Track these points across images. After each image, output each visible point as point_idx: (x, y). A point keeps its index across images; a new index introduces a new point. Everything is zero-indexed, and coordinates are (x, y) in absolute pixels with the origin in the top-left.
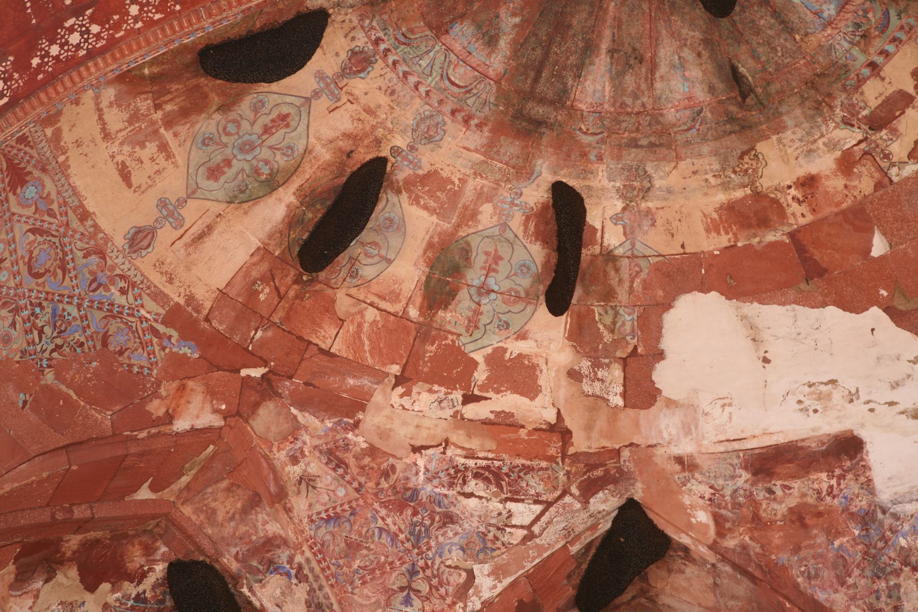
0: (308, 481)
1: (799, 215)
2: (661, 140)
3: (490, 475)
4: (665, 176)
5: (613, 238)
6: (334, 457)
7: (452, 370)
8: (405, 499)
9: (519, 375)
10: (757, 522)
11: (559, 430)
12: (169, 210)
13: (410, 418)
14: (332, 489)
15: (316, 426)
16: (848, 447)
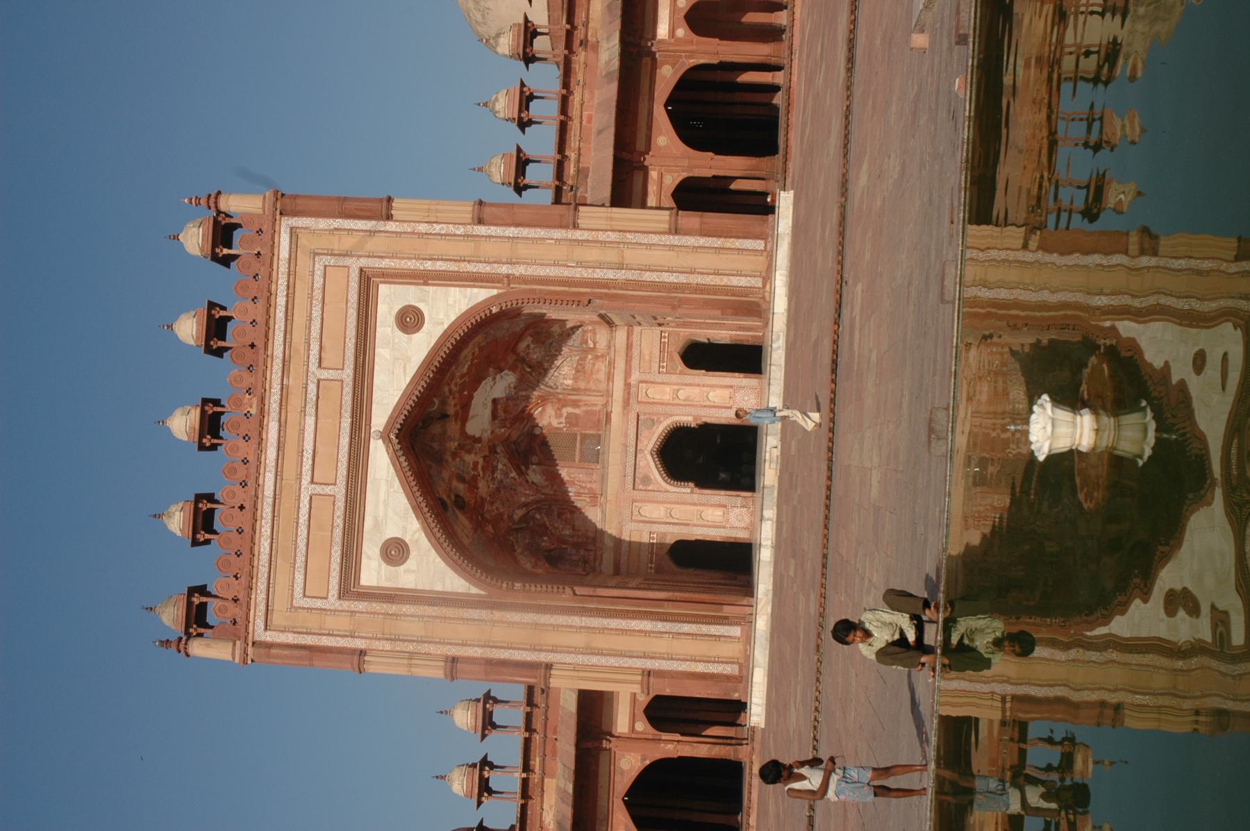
2: (444, 432)
3: (493, 472)
6: (492, 503)
7: (475, 478)
8: (498, 489)
9: (476, 464)
10: (505, 419)
11: (484, 457)
13: (483, 488)
14: (498, 504)
15: (487, 507)
16: (495, 401)
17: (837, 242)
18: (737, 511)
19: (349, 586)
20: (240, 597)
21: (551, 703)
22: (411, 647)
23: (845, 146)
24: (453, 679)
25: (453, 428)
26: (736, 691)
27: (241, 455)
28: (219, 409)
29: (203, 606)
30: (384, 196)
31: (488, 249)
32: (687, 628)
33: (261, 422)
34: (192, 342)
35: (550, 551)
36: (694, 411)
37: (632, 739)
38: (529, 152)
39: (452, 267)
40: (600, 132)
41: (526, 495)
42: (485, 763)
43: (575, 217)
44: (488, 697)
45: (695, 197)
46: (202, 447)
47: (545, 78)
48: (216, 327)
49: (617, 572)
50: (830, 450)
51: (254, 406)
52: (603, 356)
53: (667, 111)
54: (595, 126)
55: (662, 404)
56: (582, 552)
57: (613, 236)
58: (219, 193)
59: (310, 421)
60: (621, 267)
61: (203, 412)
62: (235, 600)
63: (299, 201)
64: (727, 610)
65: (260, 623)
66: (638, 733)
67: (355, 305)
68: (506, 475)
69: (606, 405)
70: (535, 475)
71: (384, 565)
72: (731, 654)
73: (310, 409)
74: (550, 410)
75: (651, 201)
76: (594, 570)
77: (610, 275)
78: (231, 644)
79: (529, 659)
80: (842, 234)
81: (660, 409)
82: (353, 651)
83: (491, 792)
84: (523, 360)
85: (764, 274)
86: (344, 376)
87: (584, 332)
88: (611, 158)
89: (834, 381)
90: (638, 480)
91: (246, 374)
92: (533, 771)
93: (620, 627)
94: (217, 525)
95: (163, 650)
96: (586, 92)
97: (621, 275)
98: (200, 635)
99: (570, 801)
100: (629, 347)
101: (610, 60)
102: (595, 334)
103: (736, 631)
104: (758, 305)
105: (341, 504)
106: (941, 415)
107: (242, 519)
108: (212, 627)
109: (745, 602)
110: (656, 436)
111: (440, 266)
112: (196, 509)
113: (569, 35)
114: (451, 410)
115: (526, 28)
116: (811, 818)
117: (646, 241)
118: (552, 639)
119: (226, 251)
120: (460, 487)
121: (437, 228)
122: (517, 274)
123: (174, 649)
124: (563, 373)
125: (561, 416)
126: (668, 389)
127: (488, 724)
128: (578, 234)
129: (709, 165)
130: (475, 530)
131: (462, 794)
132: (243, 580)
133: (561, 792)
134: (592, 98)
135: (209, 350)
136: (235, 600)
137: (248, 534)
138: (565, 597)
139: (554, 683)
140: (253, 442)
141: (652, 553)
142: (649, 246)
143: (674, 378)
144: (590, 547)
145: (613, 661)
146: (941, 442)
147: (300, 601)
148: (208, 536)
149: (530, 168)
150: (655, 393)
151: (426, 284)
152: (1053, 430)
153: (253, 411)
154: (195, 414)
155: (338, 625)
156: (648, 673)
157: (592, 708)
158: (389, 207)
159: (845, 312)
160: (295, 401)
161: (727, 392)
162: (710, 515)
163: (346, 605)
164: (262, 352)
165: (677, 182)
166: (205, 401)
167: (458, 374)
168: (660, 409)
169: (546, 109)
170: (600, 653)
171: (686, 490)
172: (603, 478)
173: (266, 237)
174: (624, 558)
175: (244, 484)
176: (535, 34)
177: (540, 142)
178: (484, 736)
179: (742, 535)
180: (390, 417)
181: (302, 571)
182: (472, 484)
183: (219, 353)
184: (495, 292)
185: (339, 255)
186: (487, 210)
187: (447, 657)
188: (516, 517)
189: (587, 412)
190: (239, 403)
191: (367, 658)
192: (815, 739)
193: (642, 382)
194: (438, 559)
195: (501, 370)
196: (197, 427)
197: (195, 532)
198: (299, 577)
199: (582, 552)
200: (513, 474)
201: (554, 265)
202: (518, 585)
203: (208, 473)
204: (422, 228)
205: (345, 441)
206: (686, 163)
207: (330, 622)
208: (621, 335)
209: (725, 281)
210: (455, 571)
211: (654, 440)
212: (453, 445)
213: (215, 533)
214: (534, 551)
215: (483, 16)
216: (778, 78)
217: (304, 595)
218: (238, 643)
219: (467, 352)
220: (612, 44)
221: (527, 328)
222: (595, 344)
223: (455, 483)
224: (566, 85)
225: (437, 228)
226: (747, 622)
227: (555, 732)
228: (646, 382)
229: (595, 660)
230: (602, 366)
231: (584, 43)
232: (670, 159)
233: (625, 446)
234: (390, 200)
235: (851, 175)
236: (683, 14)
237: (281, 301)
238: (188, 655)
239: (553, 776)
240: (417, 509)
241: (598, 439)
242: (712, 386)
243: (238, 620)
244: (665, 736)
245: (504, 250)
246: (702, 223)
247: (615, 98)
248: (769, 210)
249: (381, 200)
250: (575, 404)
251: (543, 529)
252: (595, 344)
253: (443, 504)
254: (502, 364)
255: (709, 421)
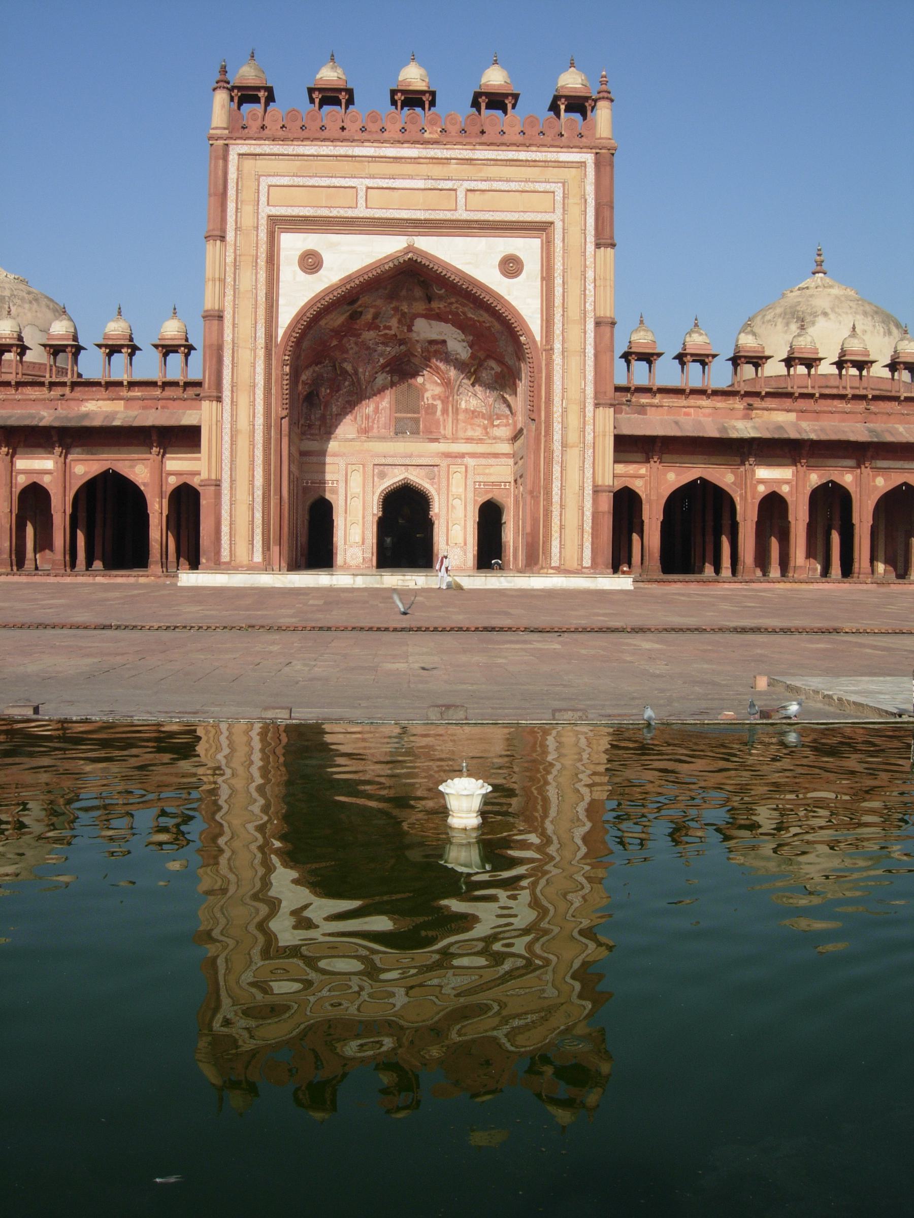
0: (352, 348)
1: (438, 311)
2: (415, 300)
3: (383, 343)
4: (415, 304)
5: (406, 310)
6: (356, 343)
7: (377, 328)
8: (368, 348)
9: (389, 328)
10: (428, 351)
11: (395, 335)
12: (332, 319)
13: (369, 336)
14: (356, 349)
15: (353, 339)
16: (444, 342)
17: (594, 626)
18: (360, 554)
19: (278, 225)
20: (266, 131)
21: (188, 402)
22: (229, 280)
23: (673, 630)
24: (204, 317)
25: (420, 307)
26: (207, 560)
27: (388, 126)
28: (427, 106)
29: (255, 100)
30: (616, 241)
31: (574, 333)
32: (258, 516)
33: (417, 142)
34: (483, 81)
35: (318, 395)
36: (443, 513)
37: (161, 474)
38: (658, 363)
39: (558, 301)
40: (676, 423)
41: (364, 372)
42: (134, 349)
43: (605, 405)
44: (190, 348)
45: (626, 505)
46: (393, 93)
47: (720, 375)
48: (497, 101)
49: (303, 454)
50: (419, 629)
51: (431, 136)
52: (487, 433)
53: (696, 480)
54: (682, 419)
55: (448, 486)
56: (318, 423)
57: (589, 438)
58: (612, 101)
59: (420, 184)
60: (564, 445)
61: (423, 92)
62: (263, 127)
63: (608, 168)
64: (275, 550)
65: (244, 149)
66: (167, 479)
67: (521, 219)
68: (381, 355)
69: (445, 437)
70: (382, 378)
71: (299, 253)
72: (238, 554)
73: (430, 184)
74: (438, 390)
75: (621, 468)
76: (303, 433)
77: (557, 437)
78: (225, 125)
79: (225, 382)
80: (600, 630)
81: (444, 483)
82: (223, 230)
83: (109, 355)
84: (480, 365)
85: (562, 567)
86: (460, 212)
87: (507, 417)
88: (655, 433)
89: (477, 629)
90: (381, 468)
91: (458, 127)
92: (129, 390)
93: (256, 459)
94: (326, 108)
95: (219, 69)
96: (710, 411)
97: (557, 446)
98: (232, 99)
99: (106, 423)
100: (496, 455)
101: (737, 430)
102: (506, 426)
103: (258, 557)
104: (536, 563)
105: (350, 213)
106: (461, 714)
107: (333, 130)
108: (239, 108)
109: (284, 564)
110: (421, 482)
111: (558, 291)
112: (339, 90)
113: (757, 394)
114: (435, 305)
115: (761, 358)
116: (110, 627)
117: (586, 466)
118: (243, 401)
119: (563, 107)
120: (368, 316)
121: (590, 287)
122: (554, 357)
123: (218, 77)
124: (474, 398)
125: (434, 399)
126: (461, 490)
127: (167, 350)
128: (590, 407)
129: (652, 517)
130: (332, 330)
131: (107, 330)
132: (281, 133)
133: (113, 415)
134: (705, 415)
135: (477, 95)
136: (263, 127)
137: (321, 135)
138: (279, 410)
139: (205, 404)
140: (399, 136)
141: (320, 483)
142: (582, 469)
143: (470, 495)
144: (322, 429)
145: (226, 454)
146: (439, 715)
147: (264, 182)
148: (317, 101)
149: (644, 365)
150: (457, 480)
151: (543, 279)
152: (464, 799)
153: (427, 135)
154: (422, 86)
155: (246, 216)
156: (218, 484)
157: (187, 438)
158: (607, 246)
159: (536, 636)
160: (437, 170)
161: (460, 540)
162: (355, 530)
163: (263, 222)
164: (478, 140)
165: (637, 491)
166: (433, 94)
167: (466, 309)
168: (444, 483)
169: (694, 376)
170: (233, 442)
171: (375, 509)
172: (383, 438)
173: (577, 141)
174: (314, 459)
175: (363, 129)
176: (757, 365)
177: (667, 373)
178: (156, 346)
179: (339, 559)
180: (426, 253)
181: (290, 183)
182: (372, 326)
183: (475, 104)
184: (538, 338)
185: (564, 204)
186: (607, 329)
187: (222, 311)
188: (345, 365)
189: (438, 422)
190: (433, 123)
191: (218, 242)
192: (176, 627)
193: (466, 467)
194: (306, 300)
195: (471, 347)
196: (411, 88)
197: (320, 90)
198: (285, 181)
199: (318, 423)
200: (382, 361)
201: (563, 388)
202: (287, 369)
203: (372, 99)
204: (590, 274)
205: (405, 215)
206: (654, 497)
207: (248, 209)
208: (506, 448)
209: (555, 535)
210: (297, 315)
211: (417, 480)
212: (405, 308)
213: (320, 107)
214: (317, 381)
215: (769, 321)
216: (726, 572)
217: (269, 186)
218: (226, 132)
219: (485, 317)
220: (750, 431)
221: (508, 367)
222: (497, 426)
223: (372, 310)
224: (716, 393)
225: (590, 287)
226: (267, 567)
227: (163, 407)
228: (466, 471)
229: (227, 438)
230: (478, 433)
231: (750, 407)
232: (657, 482)
233: (411, 456)
234: (613, 245)
235: (650, 636)
236: (776, 489)
237: (523, 155)
238: (214, 90)
239: (126, 407)
240: (349, 279)
241: (415, 432)
242: (465, 527)
243: (246, 131)
244: (165, 502)
245: (574, 343)
246: (603, 513)
247: (706, 435)
248: (616, 569)
249: (612, 238)
250: (445, 411)
251: (335, 388)
252: (496, 426)
253: (353, 302)
254: (476, 347)
255: (436, 526)
